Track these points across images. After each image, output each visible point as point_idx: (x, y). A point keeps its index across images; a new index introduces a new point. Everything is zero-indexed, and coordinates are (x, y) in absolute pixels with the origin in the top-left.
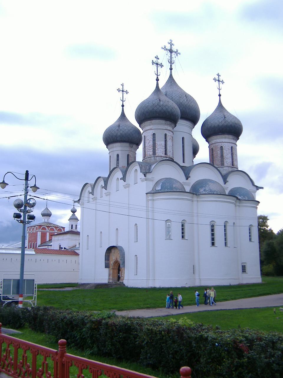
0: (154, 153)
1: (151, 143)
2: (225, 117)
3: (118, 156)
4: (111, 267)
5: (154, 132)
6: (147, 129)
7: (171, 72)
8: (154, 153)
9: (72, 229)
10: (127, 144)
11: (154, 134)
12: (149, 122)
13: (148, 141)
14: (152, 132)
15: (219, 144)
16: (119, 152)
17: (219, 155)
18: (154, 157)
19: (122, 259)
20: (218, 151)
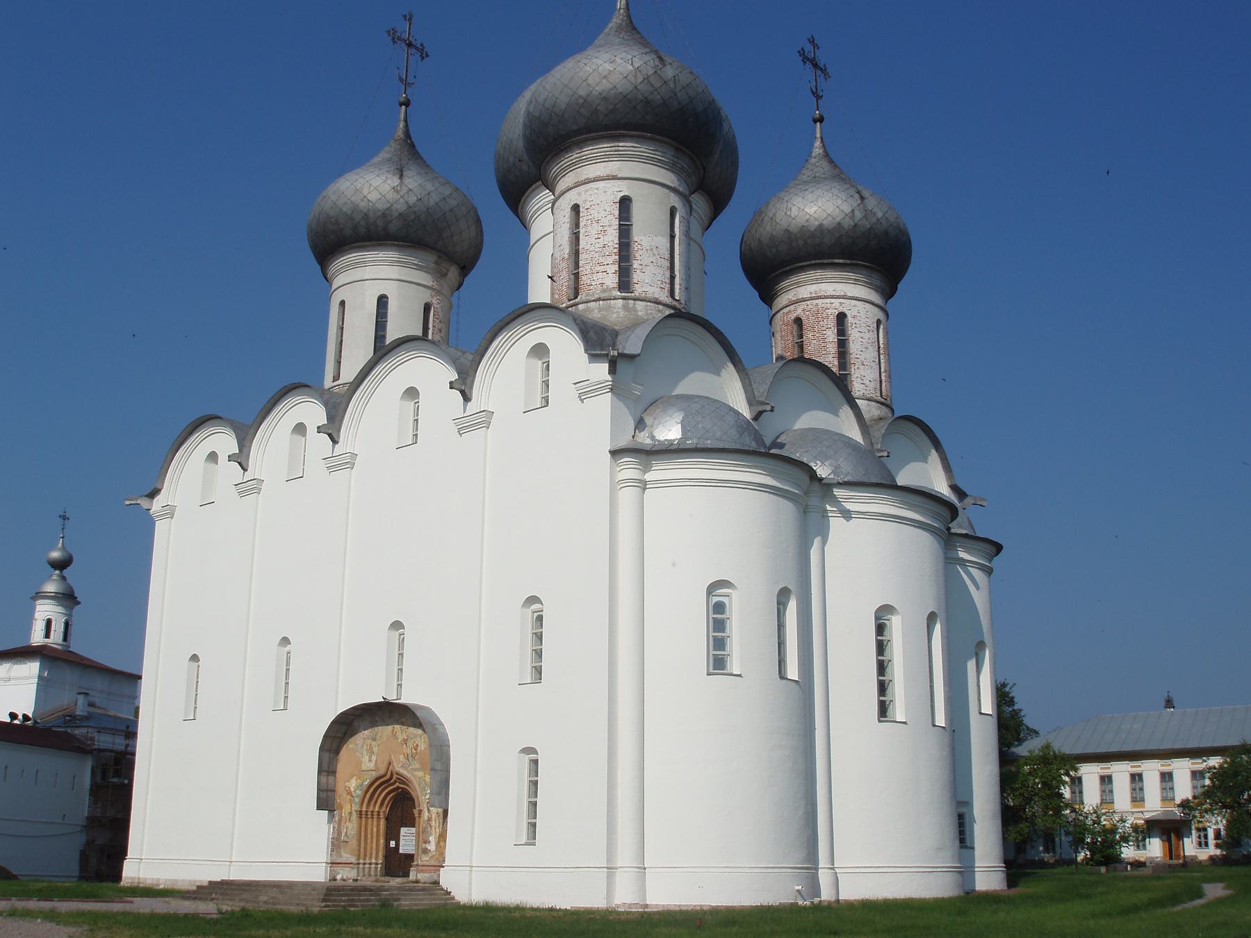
1: (612, 237)
3: (382, 301)
4: (348, 807)
5: (623, 189)
6: (591, 176)
9: (47, 635)
10: (431, 258)
14: (619, 189)
15: (828, 301)
16: (390, 290)
18: (624, 298)
19: (438, 766)
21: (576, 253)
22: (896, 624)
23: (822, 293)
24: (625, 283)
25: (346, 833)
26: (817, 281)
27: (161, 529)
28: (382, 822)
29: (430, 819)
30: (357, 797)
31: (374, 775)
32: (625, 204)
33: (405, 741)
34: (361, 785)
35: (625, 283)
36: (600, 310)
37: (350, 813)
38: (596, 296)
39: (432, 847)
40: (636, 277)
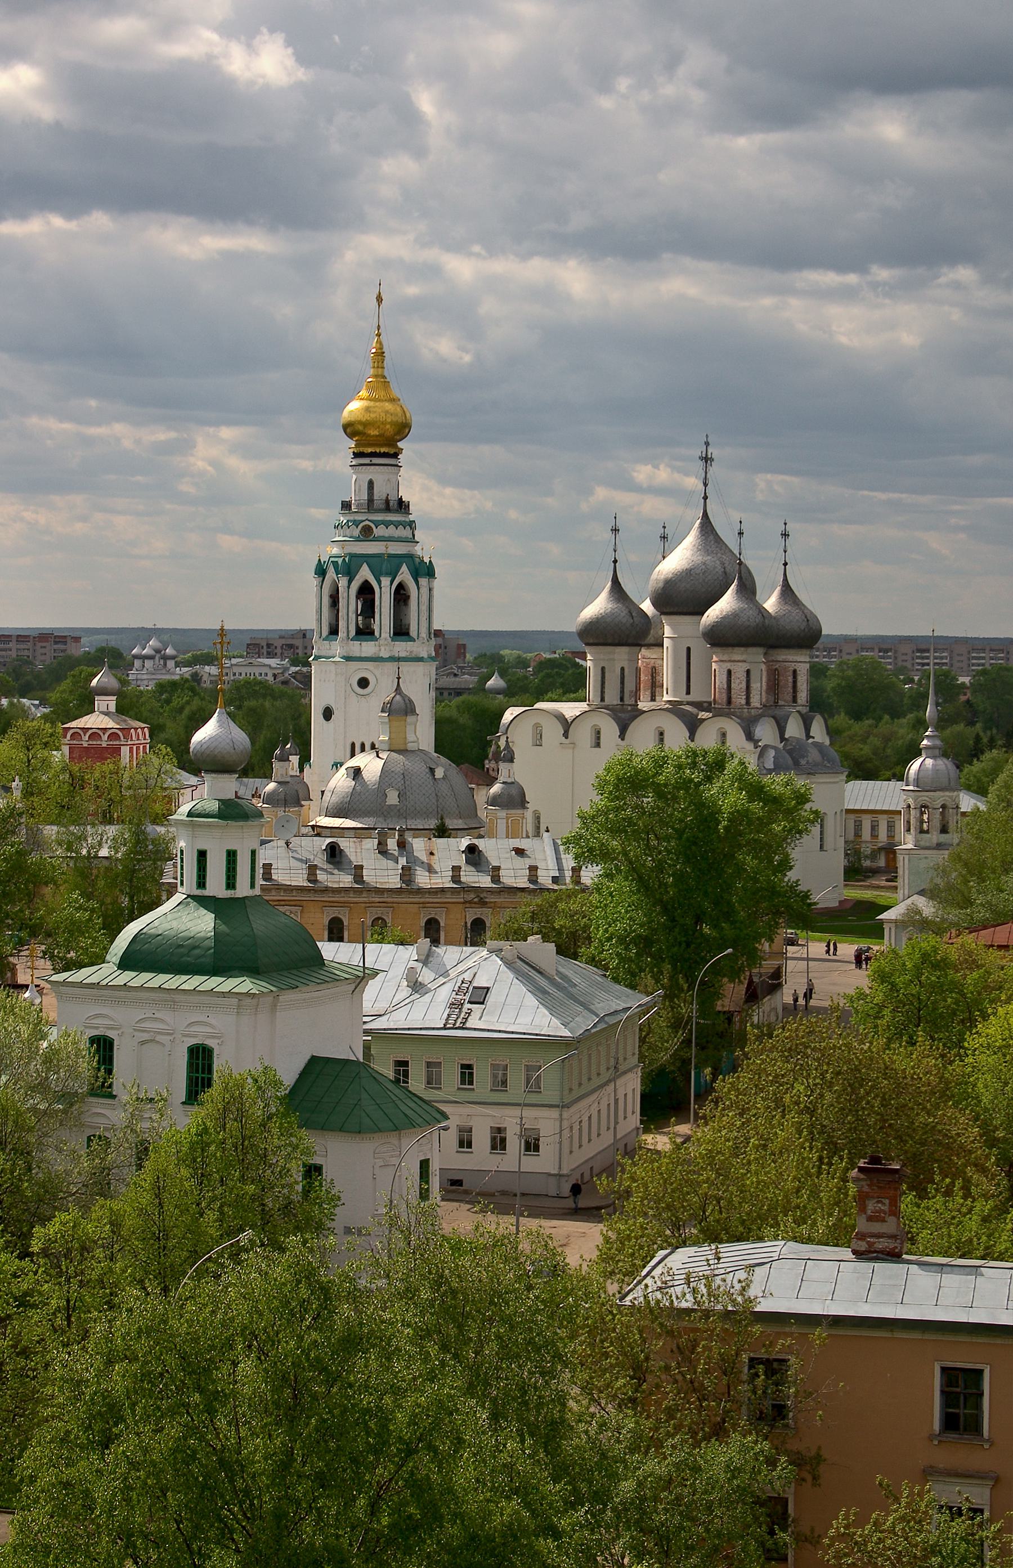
0: (748, 703)
2: (808, 620)
3: (623, 669)
6: (736, 659)
7: (705, 502)
8: (748, 703)
11: (748, 672)
13: (738, 681)
14: (745, 667)
17: (790, 685)
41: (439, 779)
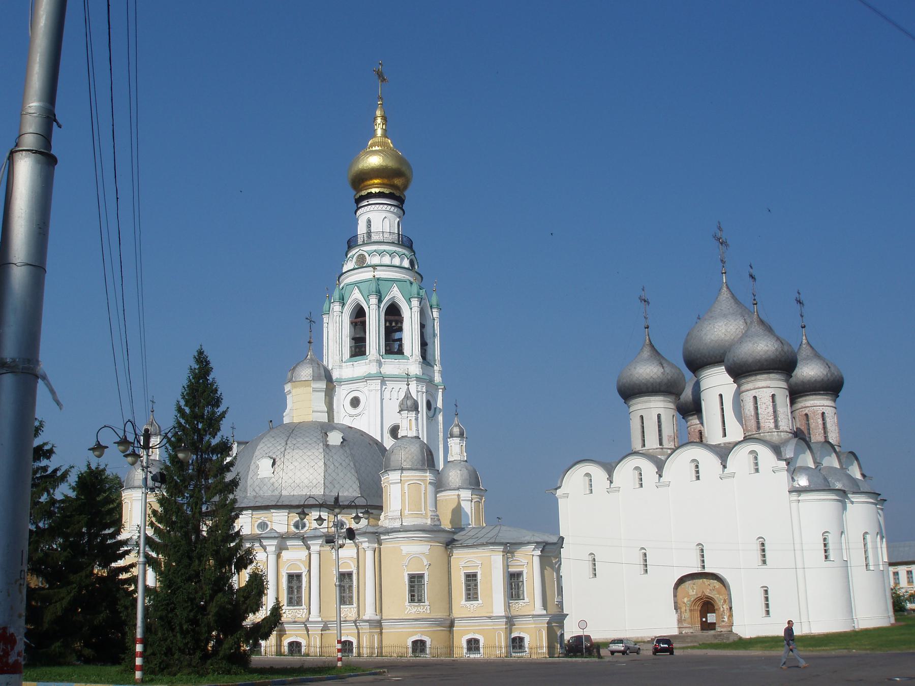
1: (771, 409)
3: (659, 416)
6: (761, 386)
12: (765, 376)
13: (764, 406)
14: (771, 392)
15: (818, 407)
16: (661, 411)
17: (821, 426)
18: (777, 432)
20: (819, 420)
21: (757, 414)
22: (868, 537)
23: (815, 405)
24: (777, 427)
25: (684, 617)
26: (813, 400)
27: (561, 503)
28: (699, 612)
29: (724, 611)
30: (688, 604)
31: (696, 597)
32: (773, 396)
33: (709, 585)
34: (690, 600)
35: (777, 427)
36: (769, 436)
37: (686, 610)
38: (768, 431)
39: (726, 619)
40: (780, 424)
41: (334, 447)
